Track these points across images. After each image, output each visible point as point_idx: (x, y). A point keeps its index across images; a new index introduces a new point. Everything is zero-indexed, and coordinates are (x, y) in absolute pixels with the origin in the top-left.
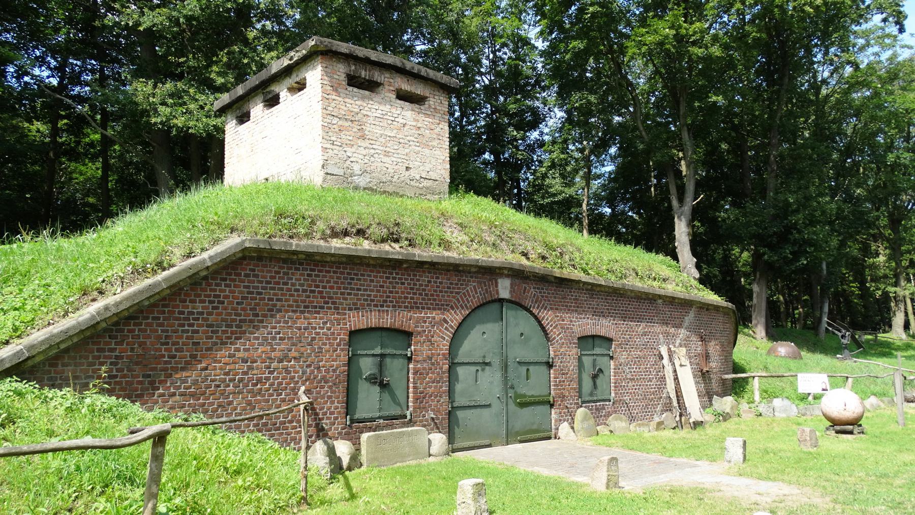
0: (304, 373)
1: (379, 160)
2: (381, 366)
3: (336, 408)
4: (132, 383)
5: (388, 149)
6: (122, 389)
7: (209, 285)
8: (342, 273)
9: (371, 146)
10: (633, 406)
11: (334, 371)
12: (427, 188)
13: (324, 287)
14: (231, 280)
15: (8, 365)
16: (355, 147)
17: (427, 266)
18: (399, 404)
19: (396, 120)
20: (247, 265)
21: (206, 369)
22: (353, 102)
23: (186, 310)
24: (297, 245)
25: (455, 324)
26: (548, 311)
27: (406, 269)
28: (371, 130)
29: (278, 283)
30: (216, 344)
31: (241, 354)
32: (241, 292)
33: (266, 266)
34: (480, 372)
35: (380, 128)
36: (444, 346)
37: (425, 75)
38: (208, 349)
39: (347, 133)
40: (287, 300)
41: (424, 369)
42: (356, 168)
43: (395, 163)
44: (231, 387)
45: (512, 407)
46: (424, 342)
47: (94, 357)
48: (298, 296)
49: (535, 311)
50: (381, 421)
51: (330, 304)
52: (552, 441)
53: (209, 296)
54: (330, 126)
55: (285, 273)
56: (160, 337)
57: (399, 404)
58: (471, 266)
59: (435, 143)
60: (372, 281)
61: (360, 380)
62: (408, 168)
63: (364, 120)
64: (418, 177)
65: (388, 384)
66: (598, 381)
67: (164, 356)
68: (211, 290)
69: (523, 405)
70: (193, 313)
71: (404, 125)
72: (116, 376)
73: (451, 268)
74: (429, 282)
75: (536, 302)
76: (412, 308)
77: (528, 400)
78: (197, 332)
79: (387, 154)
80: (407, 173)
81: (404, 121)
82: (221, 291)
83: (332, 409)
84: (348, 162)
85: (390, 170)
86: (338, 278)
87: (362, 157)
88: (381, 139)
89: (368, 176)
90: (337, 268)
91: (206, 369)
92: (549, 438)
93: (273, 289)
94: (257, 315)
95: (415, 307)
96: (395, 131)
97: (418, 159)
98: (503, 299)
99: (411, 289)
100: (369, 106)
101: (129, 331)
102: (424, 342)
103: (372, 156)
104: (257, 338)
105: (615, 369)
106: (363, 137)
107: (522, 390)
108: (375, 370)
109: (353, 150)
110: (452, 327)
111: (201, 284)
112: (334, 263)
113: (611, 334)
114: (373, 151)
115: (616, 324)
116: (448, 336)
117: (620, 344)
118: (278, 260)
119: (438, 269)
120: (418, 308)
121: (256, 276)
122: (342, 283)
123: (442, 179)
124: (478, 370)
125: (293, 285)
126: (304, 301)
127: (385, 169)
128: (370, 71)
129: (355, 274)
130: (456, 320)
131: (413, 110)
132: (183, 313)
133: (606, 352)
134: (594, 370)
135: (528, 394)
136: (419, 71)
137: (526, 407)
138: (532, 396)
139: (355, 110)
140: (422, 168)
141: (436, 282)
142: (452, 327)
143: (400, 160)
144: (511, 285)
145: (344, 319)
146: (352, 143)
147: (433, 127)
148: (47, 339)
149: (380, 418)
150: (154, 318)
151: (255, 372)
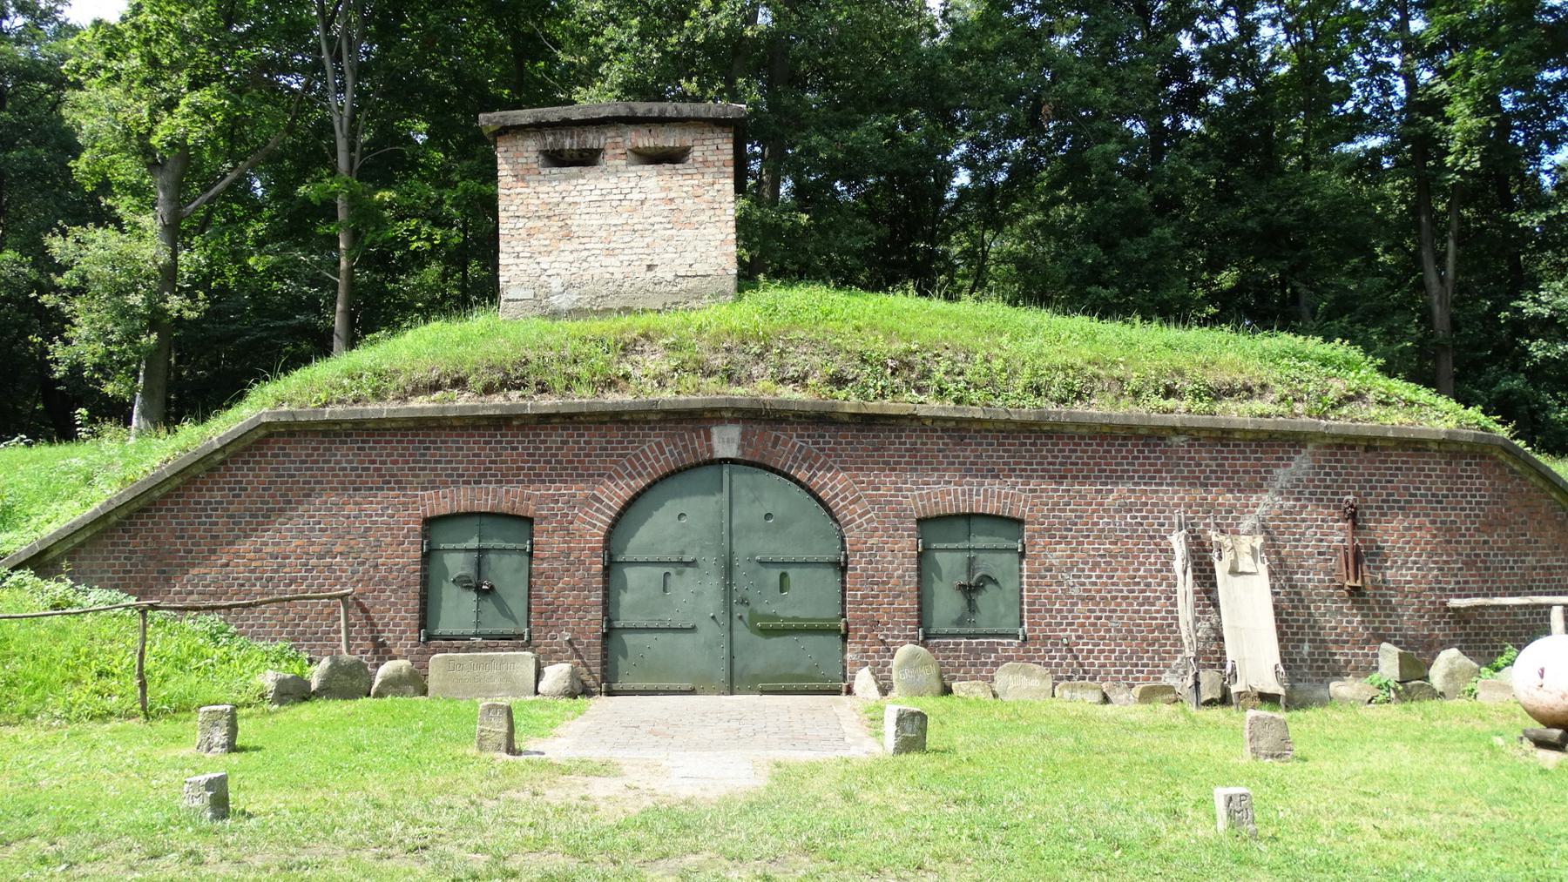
0: (354, 573)
1: (598, 265)
2: (479, 565)
3: (404, 618)
4: (147, 579)
5: (612, 245)
6: (136, 585)
7: (229, 469)
8: (409, 442)
9: (582, 247)
10: (1090, 651)
11: (399, 570)
12: (689, 291)
13: (384, 462)
14: (254, 462)
15: (23, 559)
16: (555, 253)
17: (557, 420)
18: (512, 618)
19: (628, 197)
20: (274, 443)
21: (227, 565)
22: (550, 189)
23: (203, 500)
24: (331, 413)
25: (616, 503)
26: (838, 472)
27: (518, 427)
28: (582, 222)
29: (316, 462)
30: (238, 537)
31: (269, 549)
32: (268, 476)
33: (300, 442)
34: (674, 577)
35: (598, 217)
36: (596, 536)
37: (674, 114)
38: (229, 544)
39: (541, 236)
40: (328, 482)
41: (556, 569)
42: (556, 284)
43: (626, 263)
44: (258, 587)
45: (742, 633)
46: (554, 531)
47: (108, 551)
48: (345, 476)
49: (802, 475)
50: (479, 640)
51: (393, 481)
52: (843, 698)
53: (230, 482)
54: (513, 232)
55: (325, 449)
56: (174, 530)
57: (512, 618)
58: (649, 411)
59: (704, 217)
60: (461, 449)
61: (444, 583)
62: (650, 267)
63: (570, 211)
64: (670, 277)
65: (492, 588)
66: (982, 600)
67: (179, 551)
68: (231, 476)
69: (767, 632)
70: (211, 503)
71: (642, 203)
72: (130, 571)
73: (606, 419)
74: (565, 442)
75: (804, 460)
76: (531, 482)
77: (781, 623)
78: (216, 524)
79: (611, 252)
80: (650, 274)
81: (643, 196)
82: (242, 476)
83: (397, 620)
84: (544, 278)
85: (618, 276)
86: (403, 449)
87: (568, 266)
88: (599, 233)
89: (576, 291)
90: (402, 435)
91: (227, 565)
92: (838, 692)
93: (311, 469)
94: (289, 502)
95: (539, 479)
96: (625, 215)
97: (671, 249)
98: (725, 460)
99: (532, 455)
100: (579, 188)
101: (142, 524)
102: (554, 531)
103: (585, 261)
104: (290, 530)
105: (1028, 577)
106: (568, 236)
107: (762, 609)
108: (470, 571)
109: (552, 258)
110: (610, 508)
111: (219, 469)
112: (399, 429)
113: (1021, 510)
114: (586, 253)
115: (1031, 491)
116: (602, 521)
117: (1048, 530)
118: (316, 433)
119: (582, 422)
120: (543, 482)
121: (288, 455)
122: (410, 455)
123: (720, 272)
124: (667, 574)
125: (337, 462)
126: (355, 482)
127: (608, 276)
128: (579, 136)
129: (430, 442)
130: (619, 497)
131: (659, 174)
132: (199, 503)
133: (1012, 545)
134: (969, 578)
135: (779, 613)
136: (662, 111)
137: (779, 636)
138: (795, 619)
139: (555, 200)
140: (678, 262)
141: (578, 442)
142: (610, 508)
143: (635, 257)
144: (744, 436)
145: (414, 503)
146: (550, 249)
147: (700, 192)
148: (56, 534)
149: (476, 635)
150: (167, 510)
151: (288, 569)
